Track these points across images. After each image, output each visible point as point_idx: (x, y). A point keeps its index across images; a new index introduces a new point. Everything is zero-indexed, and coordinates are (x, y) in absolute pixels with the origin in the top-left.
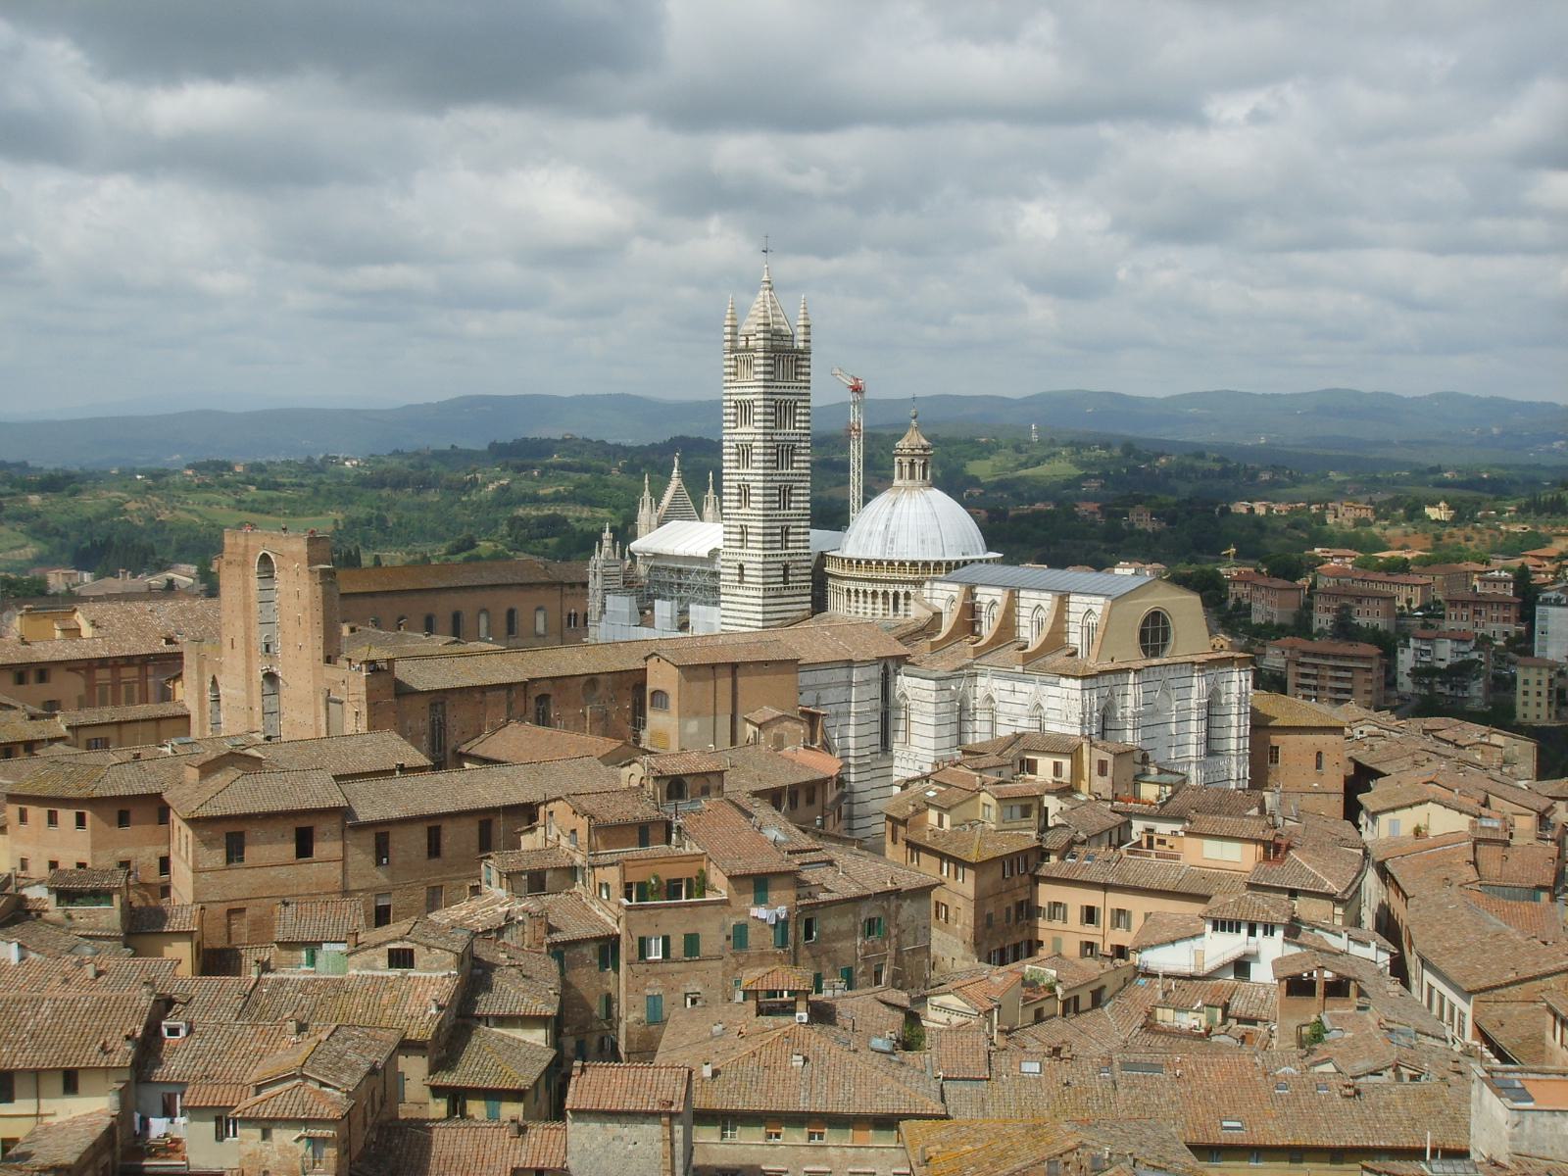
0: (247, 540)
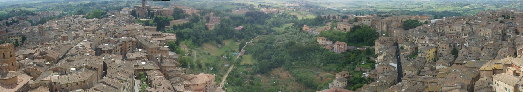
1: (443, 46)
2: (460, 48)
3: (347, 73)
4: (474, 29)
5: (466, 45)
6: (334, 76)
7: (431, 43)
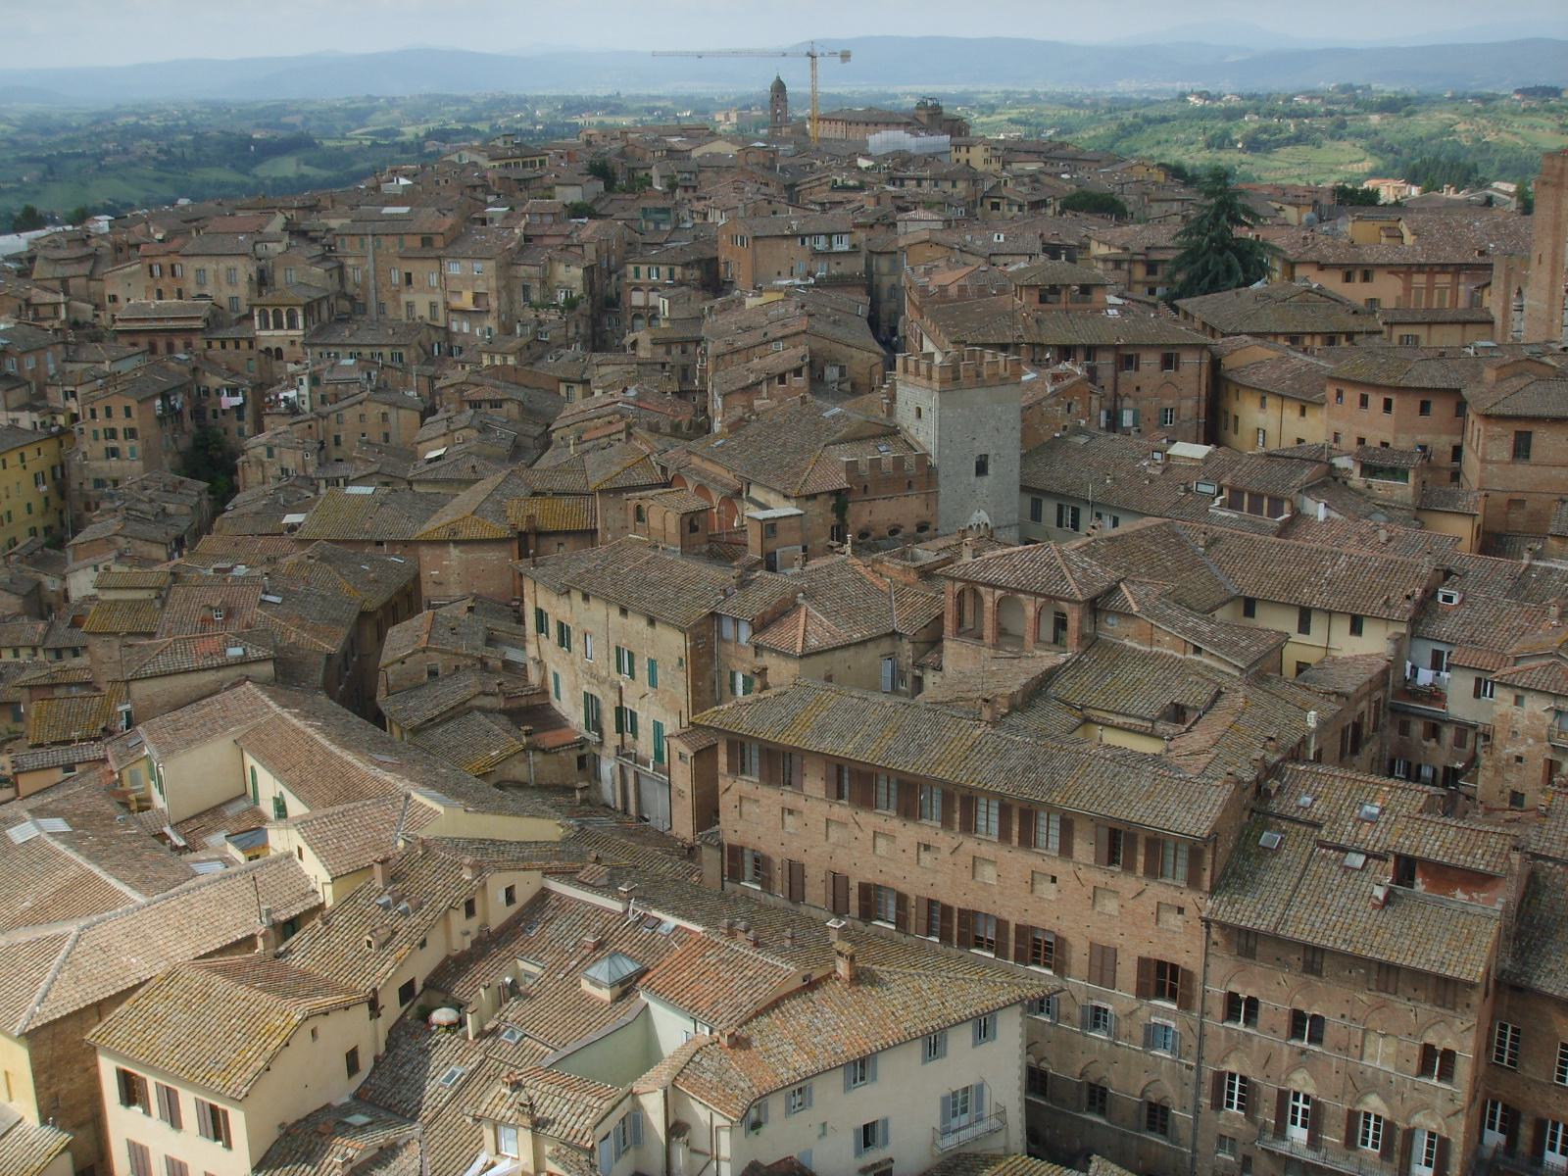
0: (1564, 163)
1: (109, 412)
2: (247, 428)
4: (354, 275)
5: (292, 394)
7: (12, 404)
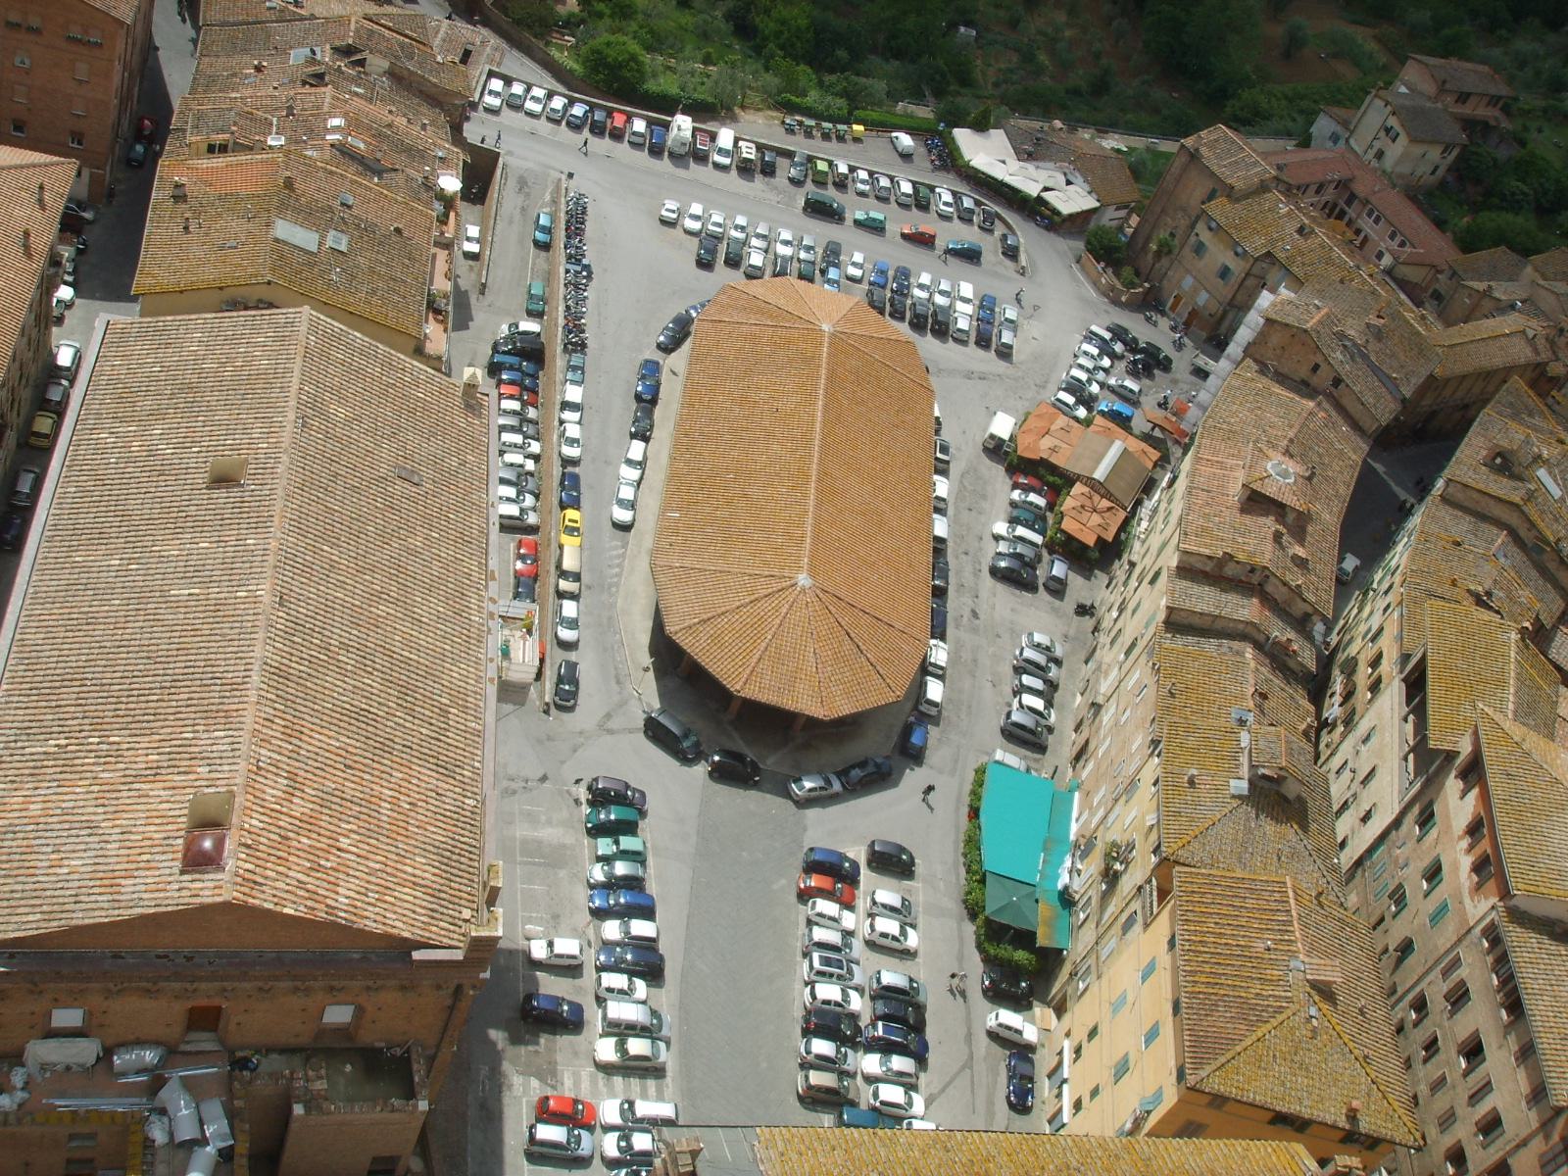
3: (1493, 90)
6: (1385, 68)
